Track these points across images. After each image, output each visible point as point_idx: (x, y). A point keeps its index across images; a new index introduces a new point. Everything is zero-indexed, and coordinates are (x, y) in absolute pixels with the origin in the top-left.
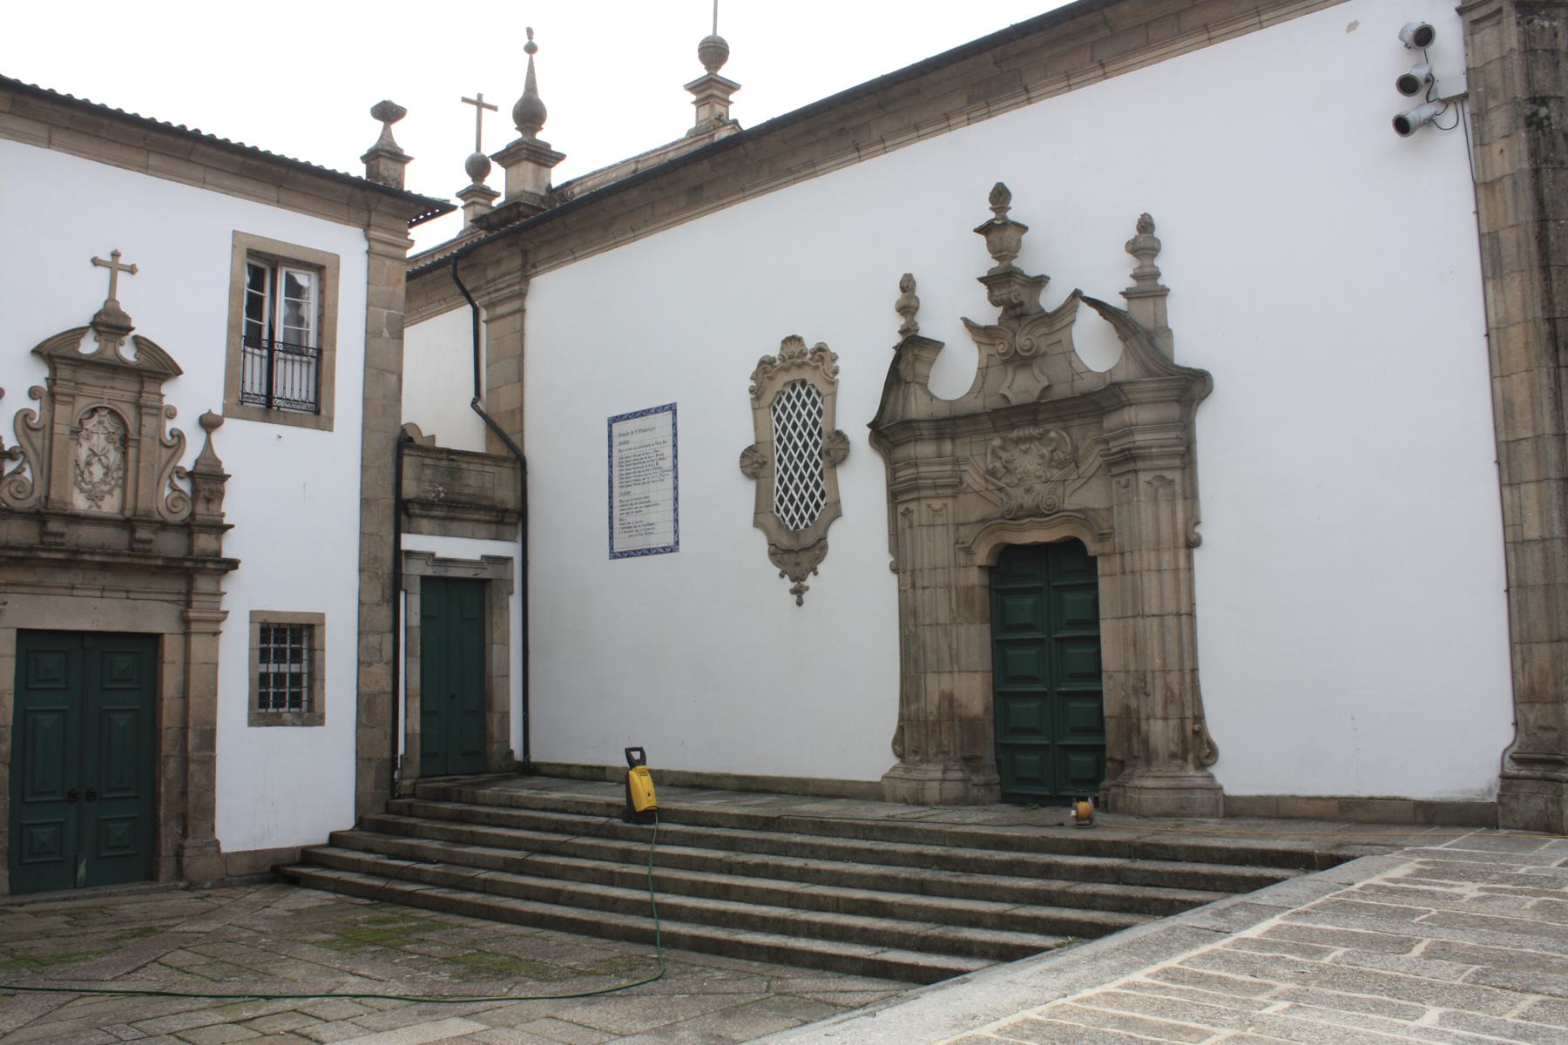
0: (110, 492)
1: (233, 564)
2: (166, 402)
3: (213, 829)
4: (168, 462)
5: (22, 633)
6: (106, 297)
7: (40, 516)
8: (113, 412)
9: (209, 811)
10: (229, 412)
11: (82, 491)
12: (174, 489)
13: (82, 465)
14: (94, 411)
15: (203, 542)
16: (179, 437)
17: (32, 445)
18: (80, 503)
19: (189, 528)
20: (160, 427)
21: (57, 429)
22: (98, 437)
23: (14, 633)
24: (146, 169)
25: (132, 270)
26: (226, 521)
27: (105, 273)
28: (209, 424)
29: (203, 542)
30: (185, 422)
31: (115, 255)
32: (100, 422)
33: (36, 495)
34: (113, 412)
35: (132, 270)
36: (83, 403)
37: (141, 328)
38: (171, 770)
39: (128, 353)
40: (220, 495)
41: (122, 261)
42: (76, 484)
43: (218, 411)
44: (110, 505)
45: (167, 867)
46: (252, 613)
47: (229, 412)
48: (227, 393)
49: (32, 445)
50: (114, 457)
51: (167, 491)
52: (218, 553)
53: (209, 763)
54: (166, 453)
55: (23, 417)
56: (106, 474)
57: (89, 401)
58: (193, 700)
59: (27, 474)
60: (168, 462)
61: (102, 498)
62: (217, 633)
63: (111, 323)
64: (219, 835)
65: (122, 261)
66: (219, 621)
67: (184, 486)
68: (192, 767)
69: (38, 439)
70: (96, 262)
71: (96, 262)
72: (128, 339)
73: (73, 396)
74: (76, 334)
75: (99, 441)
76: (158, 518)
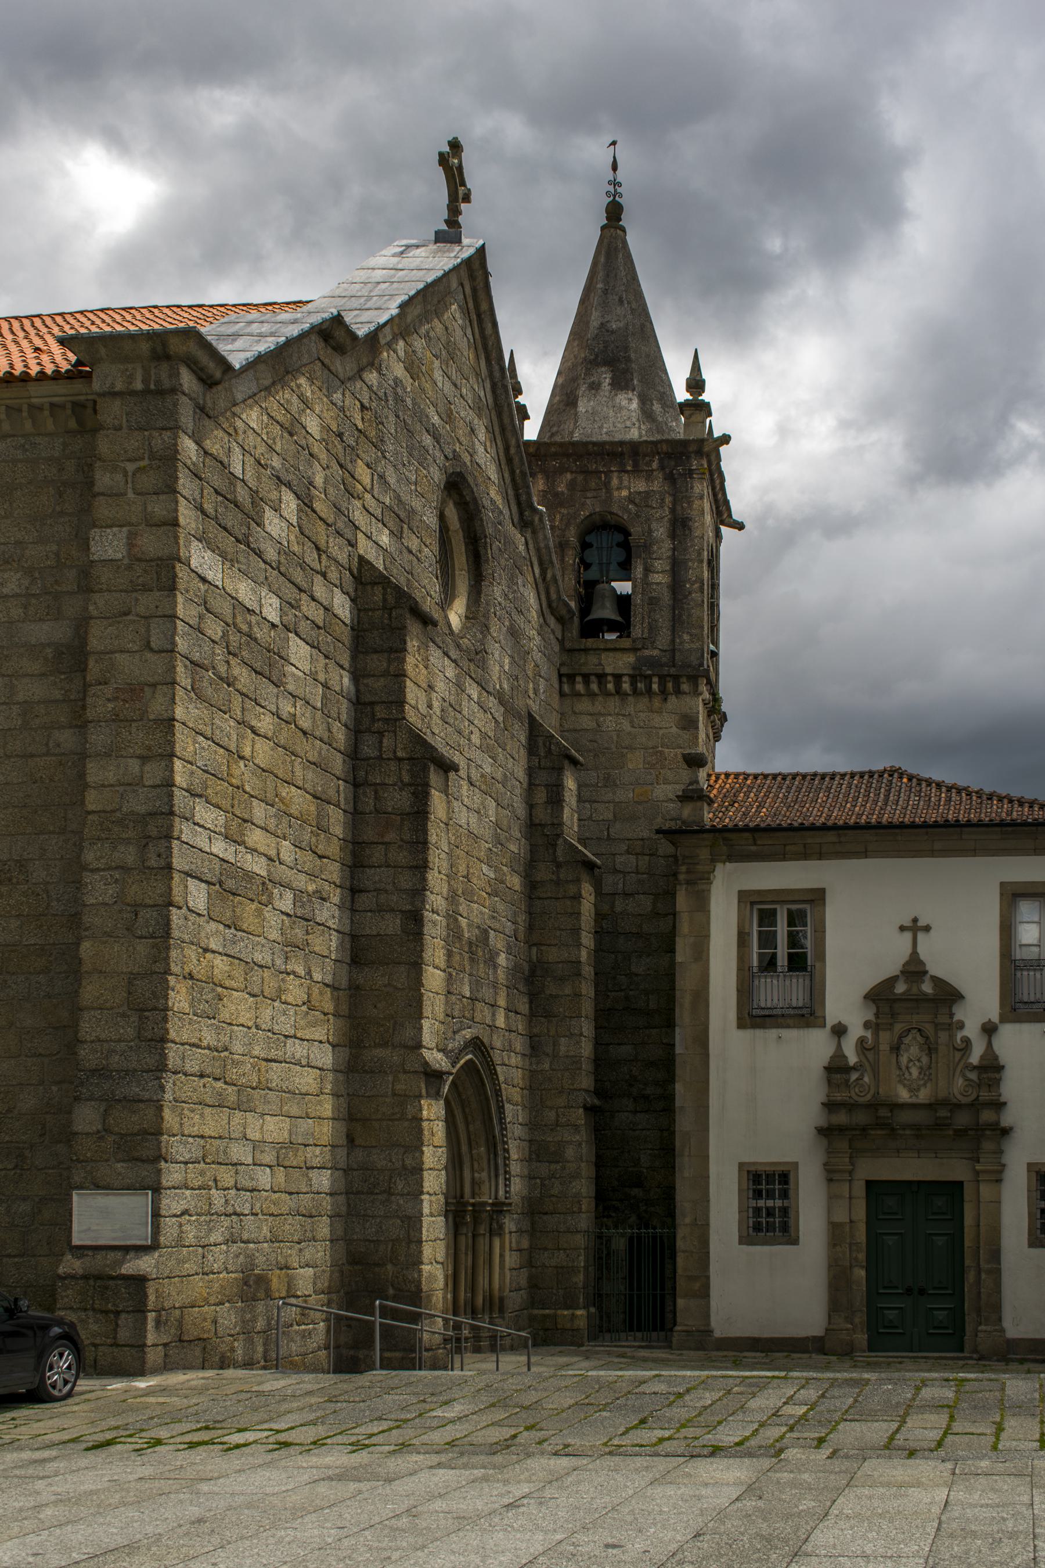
0: (925, 1085)
1: (1011, 1129)
2: (956, 1018)
3: (1000, 1319)
4: (960, 1060)
5: (870, 1185)
6: (909, 951)
7: (873, 1106)
8: (919, 1030)
9: (997, 1308)
10: (1004, 1019)
11: (905, 1086)
12: (967, 1080)
13: (904, 1068)
14: (909, 1030)
15: (987, 1116)
16: (967, 1041)
17: (868, 1061)
18: (904, 1095)
19: (975, 1106)
20: (952, 1037)
21: (881, 1047)
22: (913, 1050)
23: (863, 1184)
24: (932, 853)
25: (927, 929)
26: (1002, 1099)
27: (908, 936)
28: (989, 1030)
29: (987, 1116)
30: (972, 1030)
31: (915, 920)
32: (915, 1038)
33: (872, 1092)
34: (919, 1030)
35: (927, 929)
36: (898, 1028)
37: (935, 969)
38: (970, 1277)
39: (927, 988)
40: (998, 1082)
41: (920, 924)
42: (900, 1081)
43: (995, 1019)
44: (924, 1096)
45: (967, 1346)
46: (1029, 1165)
47: (1004, 1019)
48: (1002, 1005)
49: (868, 1061)
50: (925, 1060)
51: (961, 1081)
52: (998, 1123)
53: (996, 1273)
54: (958, 1055)
55: (861, 1041)
56: (920, 1073)
57: (903, 1025)
58: (983, 1229)
59: (866, 1079)
60: (960, 1060)
61: (918, 1090)
62: (999, 1181)
63: (914, 969)
64: (1007, 1323)
65: (920, 924)
66: (1001, 1172)
67: (973, 1076)
68: (983, 1276)
69: (870, 1055)
70: (902, 929)
71: (902, 929)
72: (927, 978)
73: (891, 1024)
74: (892, 981)
75: (914, 1051)
76: (955, 1101)
